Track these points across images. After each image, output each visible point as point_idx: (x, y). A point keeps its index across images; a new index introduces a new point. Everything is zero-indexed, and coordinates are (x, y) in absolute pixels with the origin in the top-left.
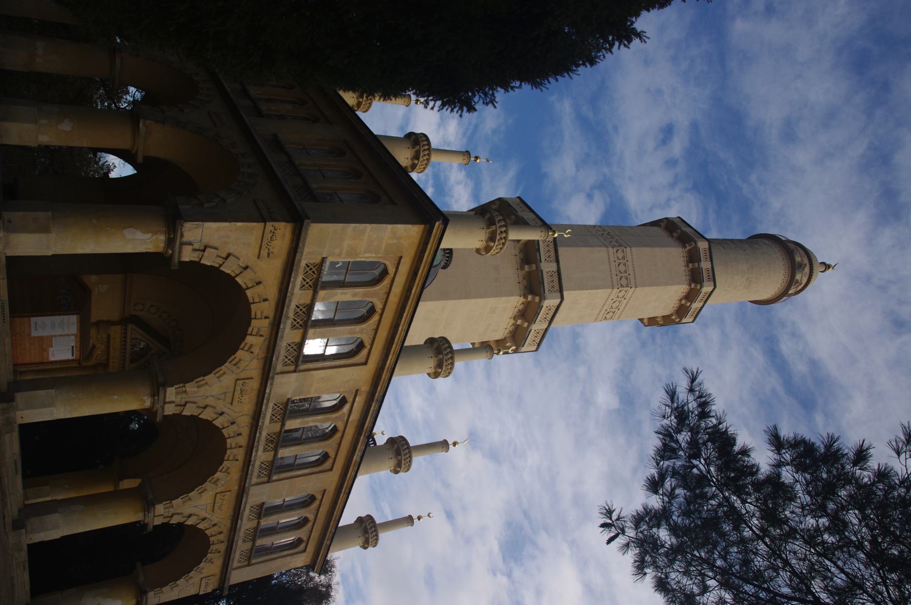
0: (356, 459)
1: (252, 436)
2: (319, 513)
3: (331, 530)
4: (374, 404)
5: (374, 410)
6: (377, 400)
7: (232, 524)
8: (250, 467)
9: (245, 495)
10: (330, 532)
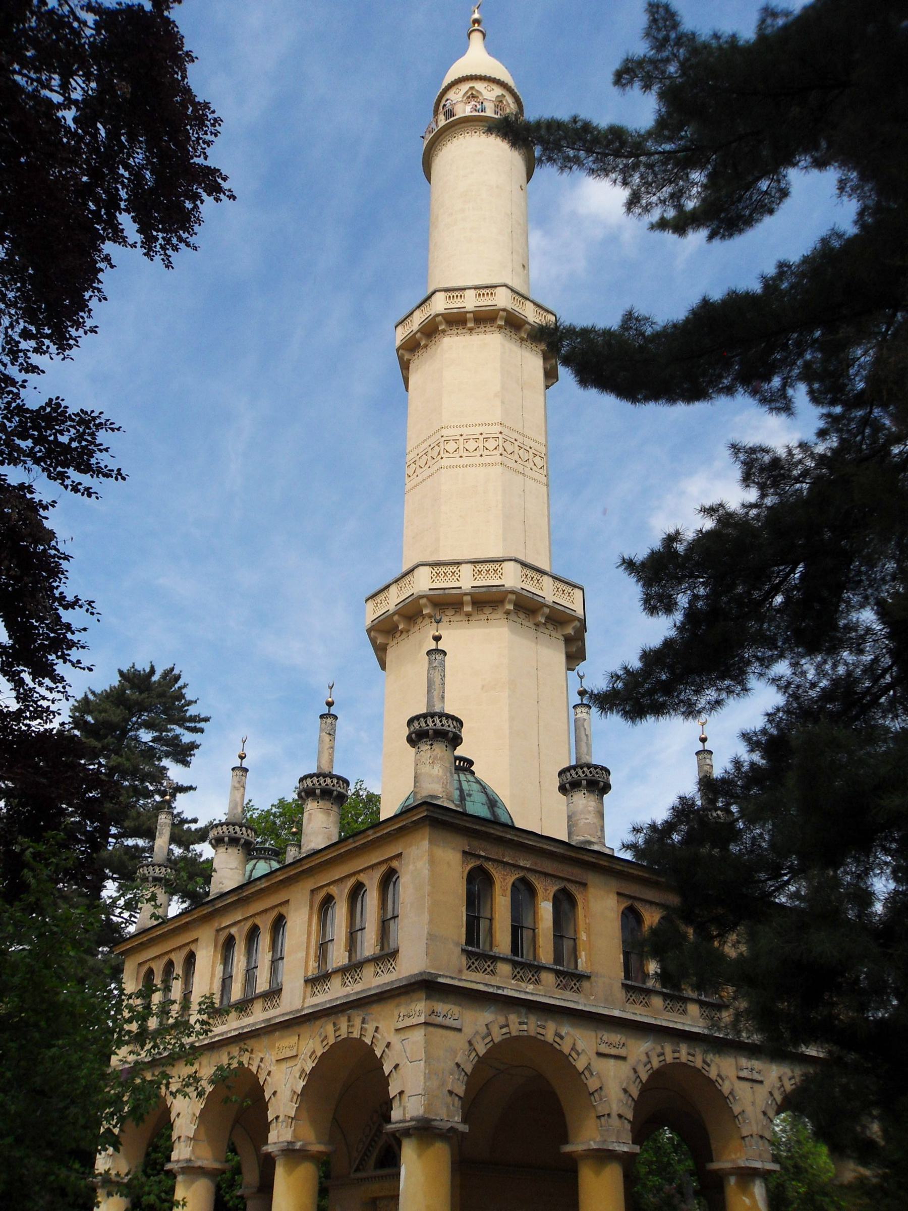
0: (265, 882)
1: (224, 1042)
3: (351, 843)
4: (217, 907)
5: (222, 902)
6: (213, 906)
8: (246, 1030)
9: (273, 1022)
10: (354, 842)
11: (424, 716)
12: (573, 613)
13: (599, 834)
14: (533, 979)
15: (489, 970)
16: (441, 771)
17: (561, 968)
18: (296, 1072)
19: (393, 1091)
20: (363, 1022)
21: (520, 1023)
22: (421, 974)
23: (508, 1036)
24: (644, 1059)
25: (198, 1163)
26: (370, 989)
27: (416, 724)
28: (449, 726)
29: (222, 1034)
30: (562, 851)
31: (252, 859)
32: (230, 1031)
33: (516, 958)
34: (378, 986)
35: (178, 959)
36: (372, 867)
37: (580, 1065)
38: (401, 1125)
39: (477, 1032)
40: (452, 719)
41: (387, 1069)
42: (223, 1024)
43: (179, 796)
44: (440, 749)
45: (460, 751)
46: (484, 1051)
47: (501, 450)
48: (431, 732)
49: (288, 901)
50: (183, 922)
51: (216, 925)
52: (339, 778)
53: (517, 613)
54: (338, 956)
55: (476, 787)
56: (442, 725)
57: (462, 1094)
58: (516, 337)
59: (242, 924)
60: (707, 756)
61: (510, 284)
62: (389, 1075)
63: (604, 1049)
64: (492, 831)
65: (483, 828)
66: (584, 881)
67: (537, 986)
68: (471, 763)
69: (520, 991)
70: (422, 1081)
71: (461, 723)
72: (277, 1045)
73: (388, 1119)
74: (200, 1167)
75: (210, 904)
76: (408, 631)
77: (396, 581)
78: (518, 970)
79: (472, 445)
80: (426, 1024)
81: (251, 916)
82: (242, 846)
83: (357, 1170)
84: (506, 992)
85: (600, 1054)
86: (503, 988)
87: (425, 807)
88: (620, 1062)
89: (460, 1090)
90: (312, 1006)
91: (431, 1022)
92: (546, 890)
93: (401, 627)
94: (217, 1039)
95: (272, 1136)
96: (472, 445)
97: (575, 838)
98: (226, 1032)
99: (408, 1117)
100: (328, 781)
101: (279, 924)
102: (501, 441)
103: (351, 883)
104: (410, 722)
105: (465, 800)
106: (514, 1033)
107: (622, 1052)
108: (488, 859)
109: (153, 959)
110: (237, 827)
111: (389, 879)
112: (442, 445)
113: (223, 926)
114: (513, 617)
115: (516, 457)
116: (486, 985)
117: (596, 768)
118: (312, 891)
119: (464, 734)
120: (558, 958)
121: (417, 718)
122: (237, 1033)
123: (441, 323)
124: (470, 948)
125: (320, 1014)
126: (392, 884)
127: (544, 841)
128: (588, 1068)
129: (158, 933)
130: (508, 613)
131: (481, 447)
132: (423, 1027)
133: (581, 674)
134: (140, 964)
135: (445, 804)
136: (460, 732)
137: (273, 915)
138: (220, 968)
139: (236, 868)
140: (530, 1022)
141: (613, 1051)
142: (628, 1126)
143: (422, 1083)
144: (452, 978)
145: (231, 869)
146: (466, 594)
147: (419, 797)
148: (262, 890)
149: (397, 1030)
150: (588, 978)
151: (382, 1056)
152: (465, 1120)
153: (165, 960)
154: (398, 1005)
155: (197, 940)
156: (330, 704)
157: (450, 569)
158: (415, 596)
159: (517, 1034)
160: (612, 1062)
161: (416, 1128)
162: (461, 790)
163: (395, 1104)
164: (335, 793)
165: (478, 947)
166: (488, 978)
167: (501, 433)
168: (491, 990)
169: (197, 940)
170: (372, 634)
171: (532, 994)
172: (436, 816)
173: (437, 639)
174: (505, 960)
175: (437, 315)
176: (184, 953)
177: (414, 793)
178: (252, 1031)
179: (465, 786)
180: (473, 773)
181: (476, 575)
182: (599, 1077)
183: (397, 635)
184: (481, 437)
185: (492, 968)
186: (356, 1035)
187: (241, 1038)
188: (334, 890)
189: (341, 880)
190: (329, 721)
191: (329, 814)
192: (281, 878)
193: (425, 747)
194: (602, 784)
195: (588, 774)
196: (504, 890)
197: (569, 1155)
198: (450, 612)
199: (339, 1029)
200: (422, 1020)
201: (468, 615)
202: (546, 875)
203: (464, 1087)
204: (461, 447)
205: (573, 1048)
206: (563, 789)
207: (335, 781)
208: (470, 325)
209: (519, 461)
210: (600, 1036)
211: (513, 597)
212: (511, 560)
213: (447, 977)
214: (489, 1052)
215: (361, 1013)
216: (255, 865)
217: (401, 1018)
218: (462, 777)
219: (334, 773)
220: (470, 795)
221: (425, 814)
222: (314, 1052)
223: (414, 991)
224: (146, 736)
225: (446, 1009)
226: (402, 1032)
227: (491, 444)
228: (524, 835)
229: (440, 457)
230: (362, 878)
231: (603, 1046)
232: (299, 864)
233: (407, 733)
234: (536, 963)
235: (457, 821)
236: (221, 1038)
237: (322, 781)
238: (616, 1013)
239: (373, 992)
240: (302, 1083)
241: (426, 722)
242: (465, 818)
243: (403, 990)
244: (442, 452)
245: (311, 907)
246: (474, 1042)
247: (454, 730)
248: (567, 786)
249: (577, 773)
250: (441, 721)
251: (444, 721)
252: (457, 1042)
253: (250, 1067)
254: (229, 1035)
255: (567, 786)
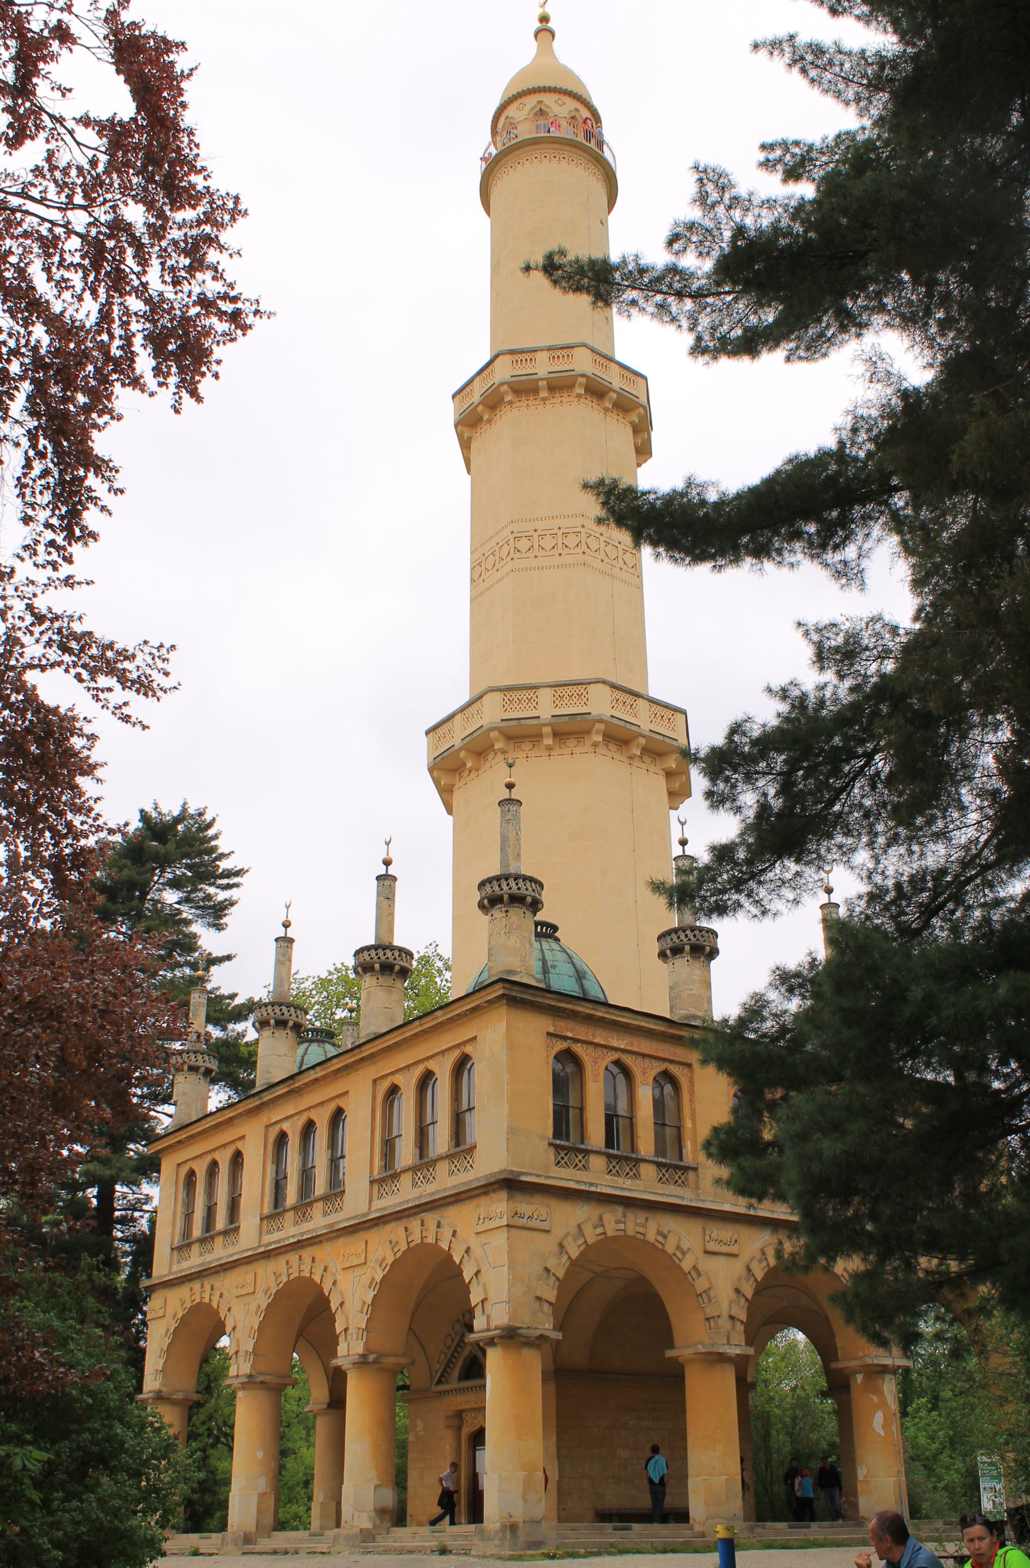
1: (283, 1250)
2: (409, 1063)
4: (265, 1099)
7: (389, 1222)
8: (305, 1237)
9: (337, 1227)
10: (421, 1025)
11: (498, 878)
12: (674, 743)
13: (706, 1006)
14: (631, 1174)
15: (580, 1165)
16: (518, 942)
17: (664, 1160)
18: (366, 1280)
19: (475, 1298)
20: (438, 1226)
21: (617, 1222)
22: (501, 1172)
23: (603, 1236)
24: (758, 1255)
25: (261, 1378)
26: (445, 1190)
27: (488, 888)
28: (527, 890)
29: (279, 1241)
30: (662, 1029)
31: (302, 1042)
32: (288, 1238)
33: (611, 1151)
34: (454, 1187)
35: (224, 1159)
36: (443, 1052)
37: (686, 1265)
38: (485, 1334)
39: (568, 1234)
40: (530, 881)
41: (467, 1276)
42: (279, 1229)
43: (214, 969)
44: (518, 916)
45: (540, 916)
46: (578, 1253)
47: (584, 548)
48: (506, 897)
49: (347, 1092)
50: (227, 1116)
51: (265, 1118)
52: (401, 950)
53: (607, 746)
54: (406, 1153)
55: (561, 956)
56: (519, 889)
57: (553, 1300)
58: (599, 408)
59: (296, 1118)
60: (833, 910)
61: (590, 343)
62: (470, 1282)
63: (712, 1246)
64: (580, 1009)
65: (570, 1006)
66: (688, 1062)
67: (636, 1181)
68: (555, 928)
69: (616, 1188)
70: (507, 1287)
71: (541, 885)
72: (342, 1252)
73: (470, 1328)
74: (262, 1382)
75: (257, 1098)
76: (477, 770)
77: (462, 709)
78: (614, 1163)
79: (548, 542)
80: (508, 1226)
81: (305, 1110)
82: (292, 1028)
83: (439, 1382)
84: (599, 1190)
85: (707, 1252)
86: (596, 1185)
87: (500, 985)
88: (732, 1260)
89: (551, 1295)
90: (381, 1209)
91: (514, 1224)
92: (644, 1074)
93: (469, 765)
94: (273, 1247)
95: (342, 1349)
96: (548, 542)
97: (678, 1012)
98: (283, 1239)
99: (493, 1326)
100: (389, 953)
101: (338, 1117)
102: (584, 536)
103: (418, 1071)
104: (482, 885)
105: (549, 972)
106: (610, 1233)
107: (733, 1249)
108: (576, 1041)
109: (194, 1158)
110: (284, 1008)
111: (462, 1065)
112: (511, 542)
113: (274, 1120)
114: (601, 750)
115: (603, 556)
116: (577, 1182)
117: (700, 931)
118: (375, 1081)
119: (545, 897)
120: (660, 1149)
121: (489, 880)
122: (296, 1240)
123: (506, 393)
124: (558, 1142)
125: (389, 1218)
126: (466, 1072)
127: (639, 1017)
128: (695, 1268)
129: (198, 1130)
130: (595, 745)
131: (560, 545)
132: (506, 1229)
133: (683, 820)
134: (179, 1165)
135: (524, 981)
136: (540, 895)
137: (331, 1108)
138: (271, 1169)
139: (285, 1055)
140: (627, 1220)
141: (724, 1249)
142: (740, 1328)
143: (506, 1289)
144: (538, 1176)
145: (280, 1056)
146: (545, 725)
147: (493, 972)
148: (316, 1080)
149: (477, 1233)
150: (695, 1169)
151: (461, 1262)
152: (559, 1326)
153: (208, 1159)
154: (478, 1206)
155: (243, 1137)
156: (387, 863)
157: (525, 695)
158: (484, 729)
159: (614, 1234)
160: (723, 1260)
161: (501, 1337)
162: (544, 961)
163: (478, 1312)
164: (397, 968)
165: (568, 1139)
166: (580, 1175)
167: (583, 526)
168: (583, 1187)
169: (243, 1137)
170: (435, 773)
171: (630, 1190)
172: (514, 994)
173: (510, 786)
174: (598, 1153)
175: (502, 384)
176: (229, 1152)
177: (488, 967)
178: (312, 1238)
179: (548, 955)
180: (557, 940)
181: (557, 702)
182: (708, 1277)
183: (465, 774)
184: (559, 533)
185: (583, 1162)
186: (431, 1240)
187: (299, 1245)
188: (399, 1079)
189: (408, 1067)
190: (387, 883)
191: (391, 992)
192: (338, 1066)
193: (497, 912)
194: (708, 949)
195: (692, 938)
196: (595, 1076)
197: (674, 1360)
198: (527, 746)
199: (412, 1233)
200: (504, 1222)
201: (549, 748)
202: (644, 1056)
203: (555, 1292)
204: (536, 546)
205: (678, 1248)
206: (662, 955)
207: (397, 953)
208: (544, 394)
209: (606, 560)
210: (708, 1233)
211: (601, 727)
212: (598, 682)
213: (531, 1174)
214: (582, 1254)
215: (436, 1216)
216: (307, 1050)
217: (482, 1220)
218: (545, 945)
219: (395, 944)
220: (554, 967)
221: (501, 992)
222: (384, 1259)
223: (494, 1191)
224: (171, 897)
225: (530, 1207)
226: (483, 1235)
227: (572, 541)
228: (618, 1012)
229: (510, 557)
230: (432, 1065)
231: (712, 1243)
232: (358, 1051)
233: (479, 898)
234: (634, 1156)
235: (538, 999)
236: (278, 1245)
237: (381, 954)
238: (727, 1207)
239: (448, 1193)
240: (372, 1294)
241: (499, 886)
242: (548, 995)
243: (483, 1190)
244: (512, 551)
245: (374, 1099)
246: (565, 1243)
247: (533, 894)
248: (668, 952)
249: (679, 937)
250: (517, 884)
251: (521, 884)
252: (547, 1244)
253: (313, 1276)
254: (287, 1242)
255: (668, 952)
